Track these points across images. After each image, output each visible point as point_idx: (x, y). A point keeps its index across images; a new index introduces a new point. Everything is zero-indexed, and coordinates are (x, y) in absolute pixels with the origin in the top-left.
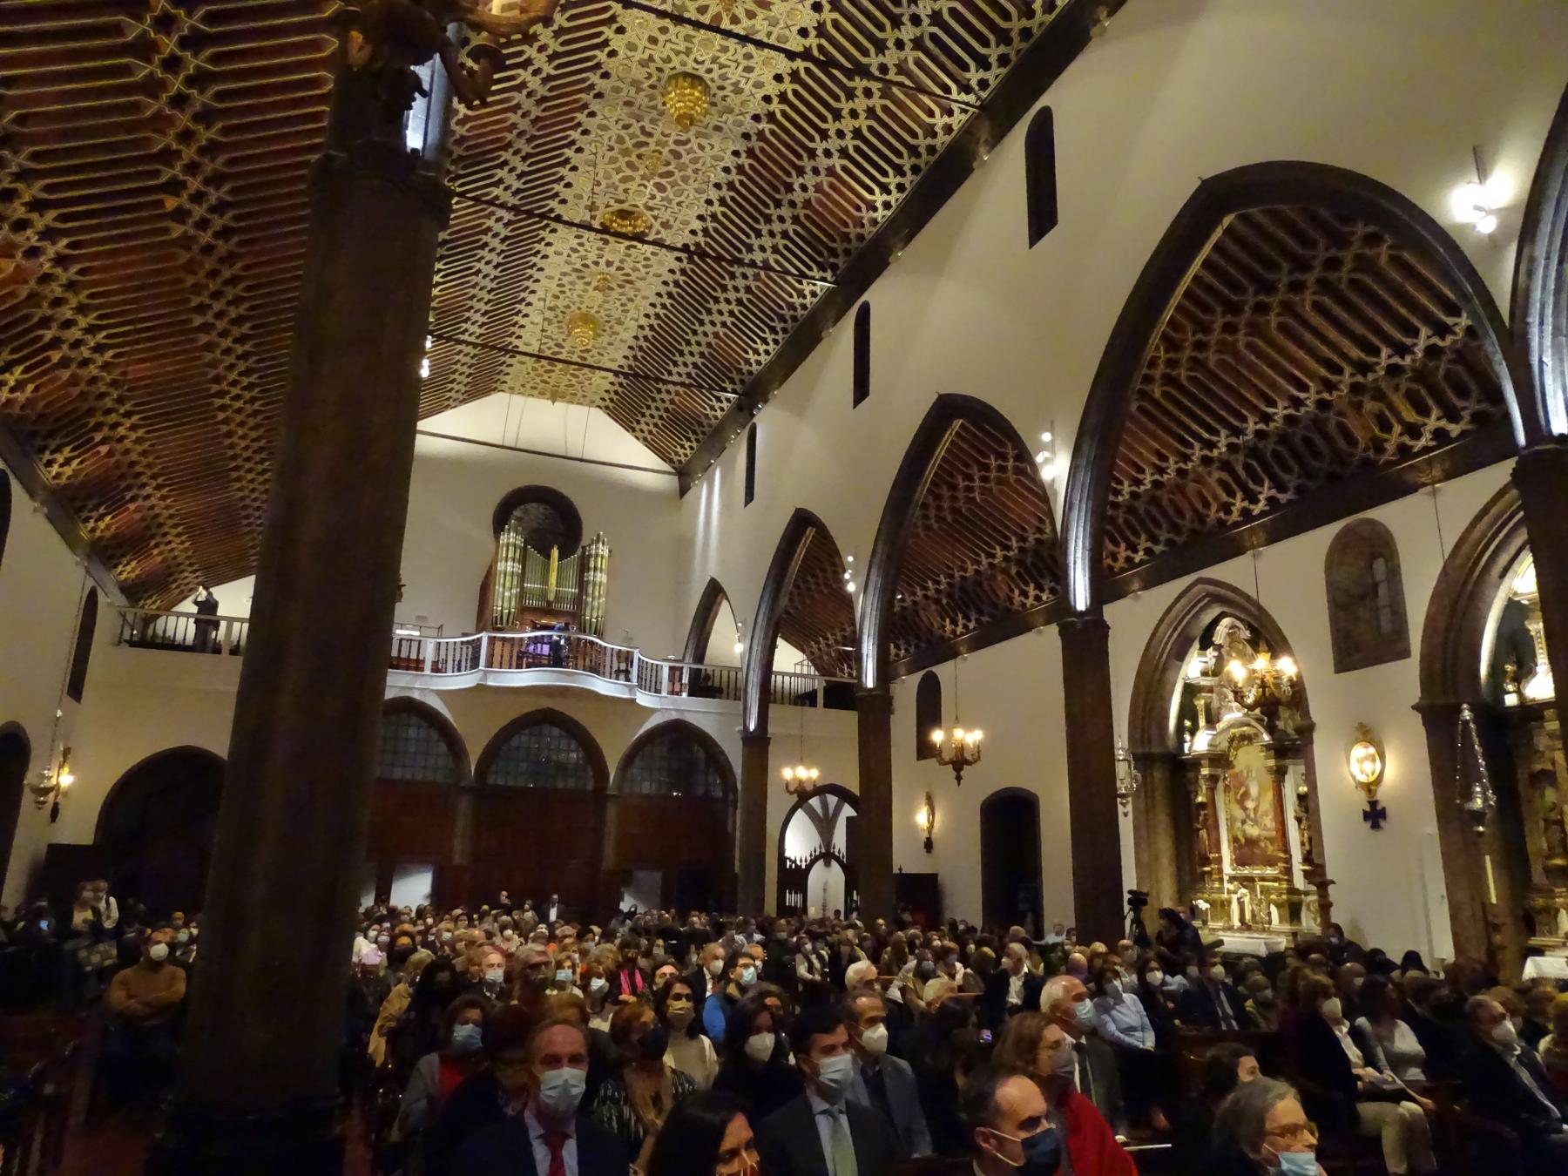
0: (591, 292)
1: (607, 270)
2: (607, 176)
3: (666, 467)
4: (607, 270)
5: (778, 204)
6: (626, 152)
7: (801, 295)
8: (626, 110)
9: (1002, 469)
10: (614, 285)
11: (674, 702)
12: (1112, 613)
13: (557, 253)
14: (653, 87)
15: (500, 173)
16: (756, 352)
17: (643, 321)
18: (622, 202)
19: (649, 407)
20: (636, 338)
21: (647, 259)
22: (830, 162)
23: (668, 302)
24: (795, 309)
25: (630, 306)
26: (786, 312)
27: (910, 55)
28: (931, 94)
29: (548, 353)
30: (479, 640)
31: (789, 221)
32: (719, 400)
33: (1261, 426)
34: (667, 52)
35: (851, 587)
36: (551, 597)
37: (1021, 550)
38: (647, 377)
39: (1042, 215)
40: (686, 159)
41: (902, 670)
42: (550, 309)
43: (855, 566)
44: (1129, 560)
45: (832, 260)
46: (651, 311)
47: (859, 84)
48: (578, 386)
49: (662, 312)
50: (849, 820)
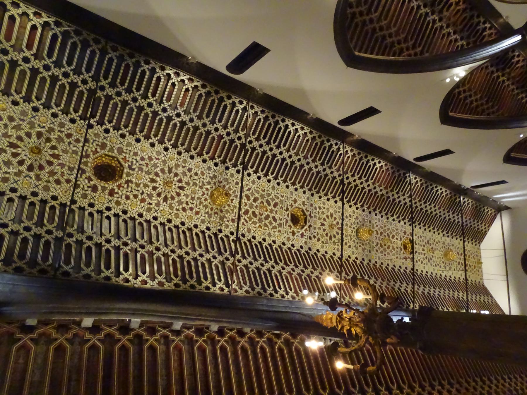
0: (435, 255)
1: (426, 250)
2: (394, 255)
3: (498, 217)
4: (426, 250)
5: (388, 197)
6: (385, 250)
7: (417, 182)
8: (372, 252)
9: (464, 91)
10: (431, 247)
12: (517, 24)
13: (424, 268)
14: (363, 245)
15: (403, 290)
16: (442, 193)
17: (441, 235)
18: (401, 249)
19: (475, 227)
20: (448, 236)
21: (418, 237)
22: (371, 184)
24: (422, 183)
25: (436, 240)
27: (334, 169)
28: (343, 159)
29: (463, 267)
31: (393, 193)
32: (464, 202)
33: (422, 7)
34: (352, 242)
37: (497, 71)
38: (463, 230)
39: (371, 112)
40: (382, 230)
42: (445, 268)
44: (490, 28)
45: (402, 175)
47: (346, 181)
48: (473, 255)
49: (436, 229)
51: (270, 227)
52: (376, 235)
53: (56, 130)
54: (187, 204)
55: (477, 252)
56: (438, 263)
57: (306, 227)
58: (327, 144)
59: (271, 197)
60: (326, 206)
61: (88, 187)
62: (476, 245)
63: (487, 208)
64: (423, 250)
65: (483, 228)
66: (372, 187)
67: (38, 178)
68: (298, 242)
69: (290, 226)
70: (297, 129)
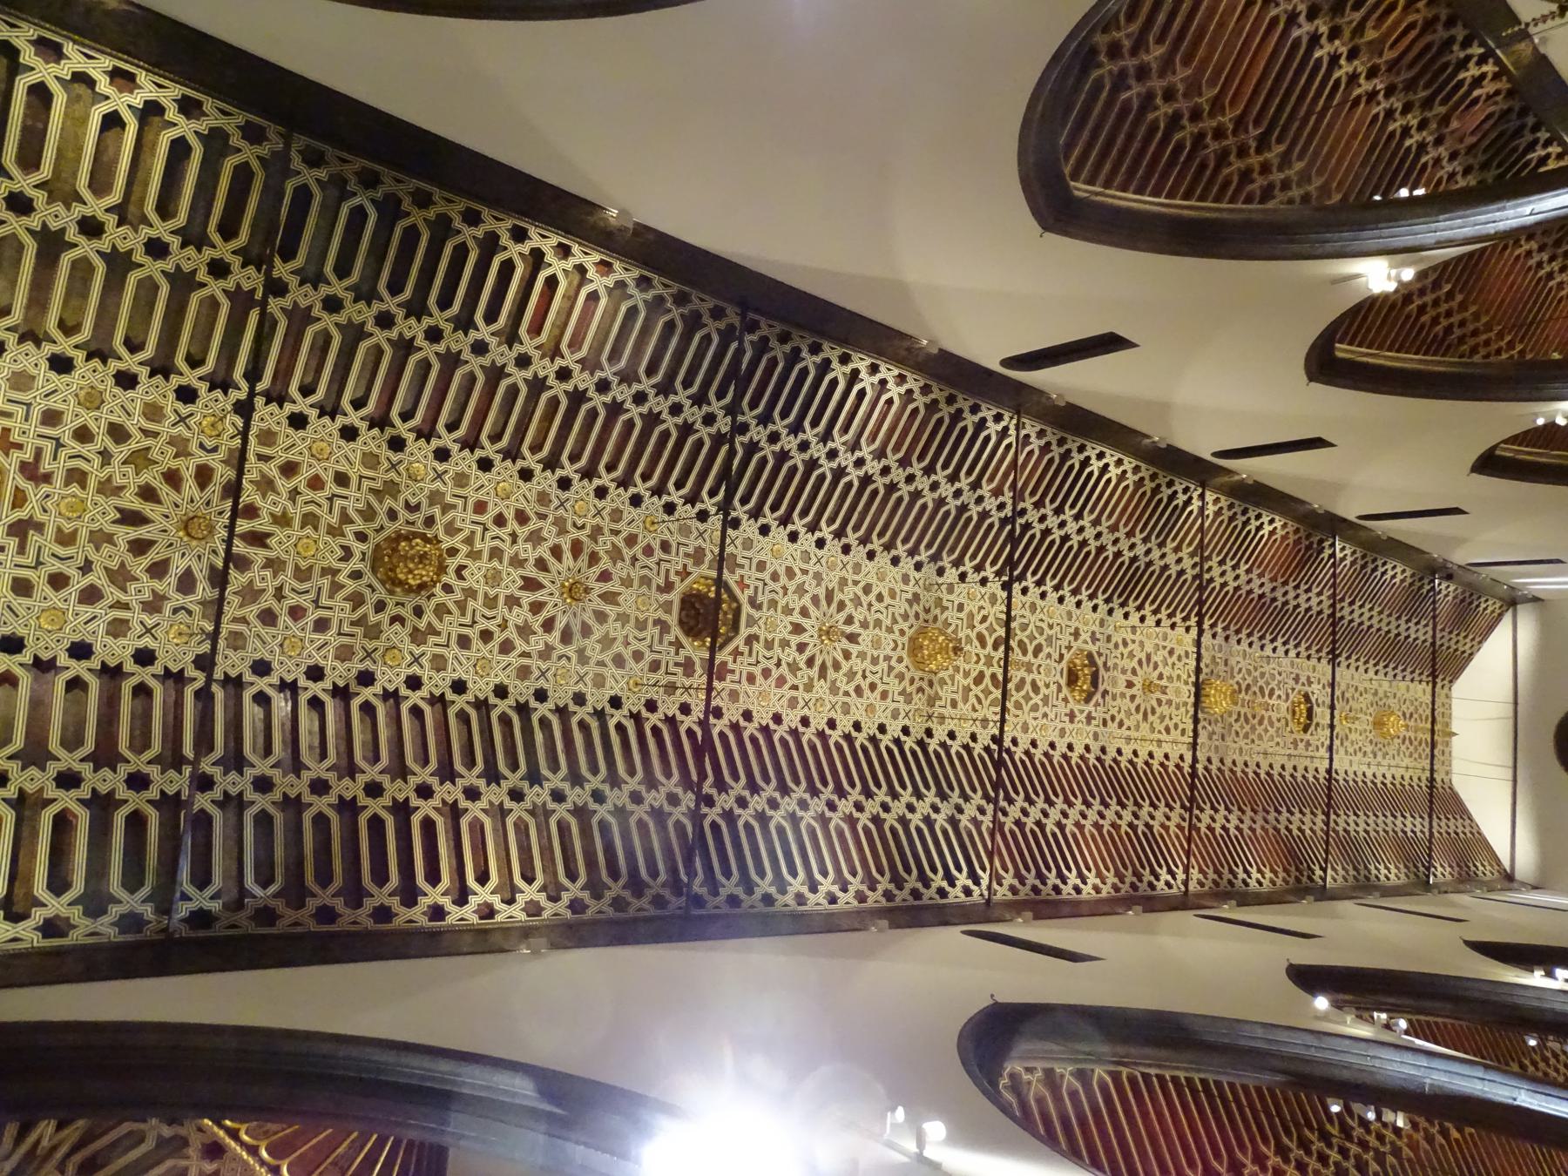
3: (1507, 619)
5: (1274, 600)
6: (1253, 728)
16: (1394, 577)
23: (1354, 657)
25: (1361, 689)
26: (1360, 562)
40: (1249, 680)
46: (1362, 669)
51: (1026, 708)
53: (606, 531)
54: (864, 677)
57: (1098, 697)
58: (1166, 492)
59: (1027, 632)
60: (1137, 637)
61: (677, 664)
67: (583, 659)
68: (1081, 736)
69: (1065, 700)
70: (1114, 467)
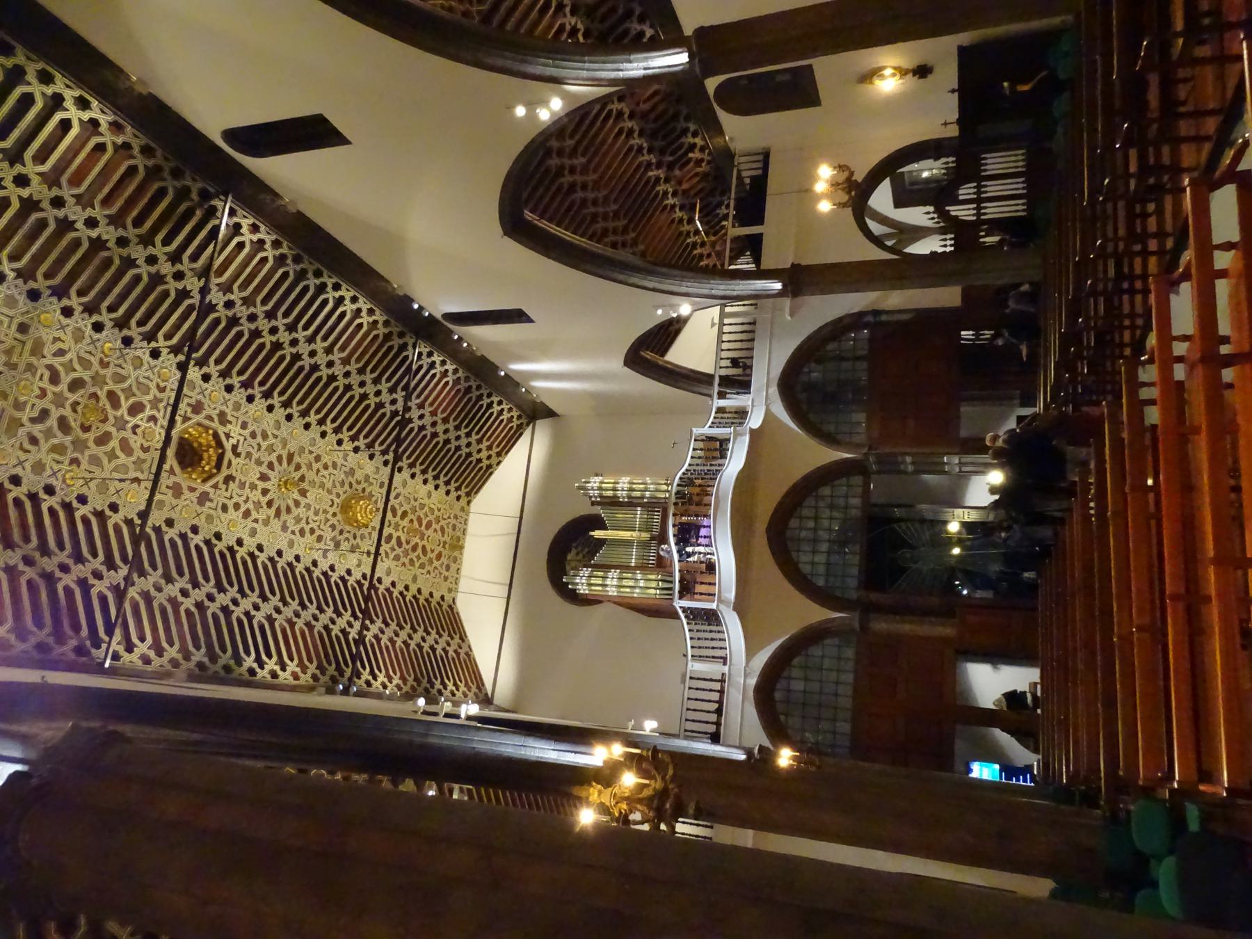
1: (274, 481)
10: (297, 475)
11: (759, 391)
21: (253, 435)
25: (326, 459)
26: (291, 268)
30: (684, 610)
35: (557, 104)
36: (645, 535)
41: (718, 141)
42: (337, 545)
43: (531, 105)
45: (194, 196)
48: (442, 523)
50: (898, 204)
52: (45, 384)
55: (456, 517)
56: (314, 525)
62: (458, 498)
63: (500, 403)
64: (264, 478)
65: (484, 454)
66: (37, 189)
